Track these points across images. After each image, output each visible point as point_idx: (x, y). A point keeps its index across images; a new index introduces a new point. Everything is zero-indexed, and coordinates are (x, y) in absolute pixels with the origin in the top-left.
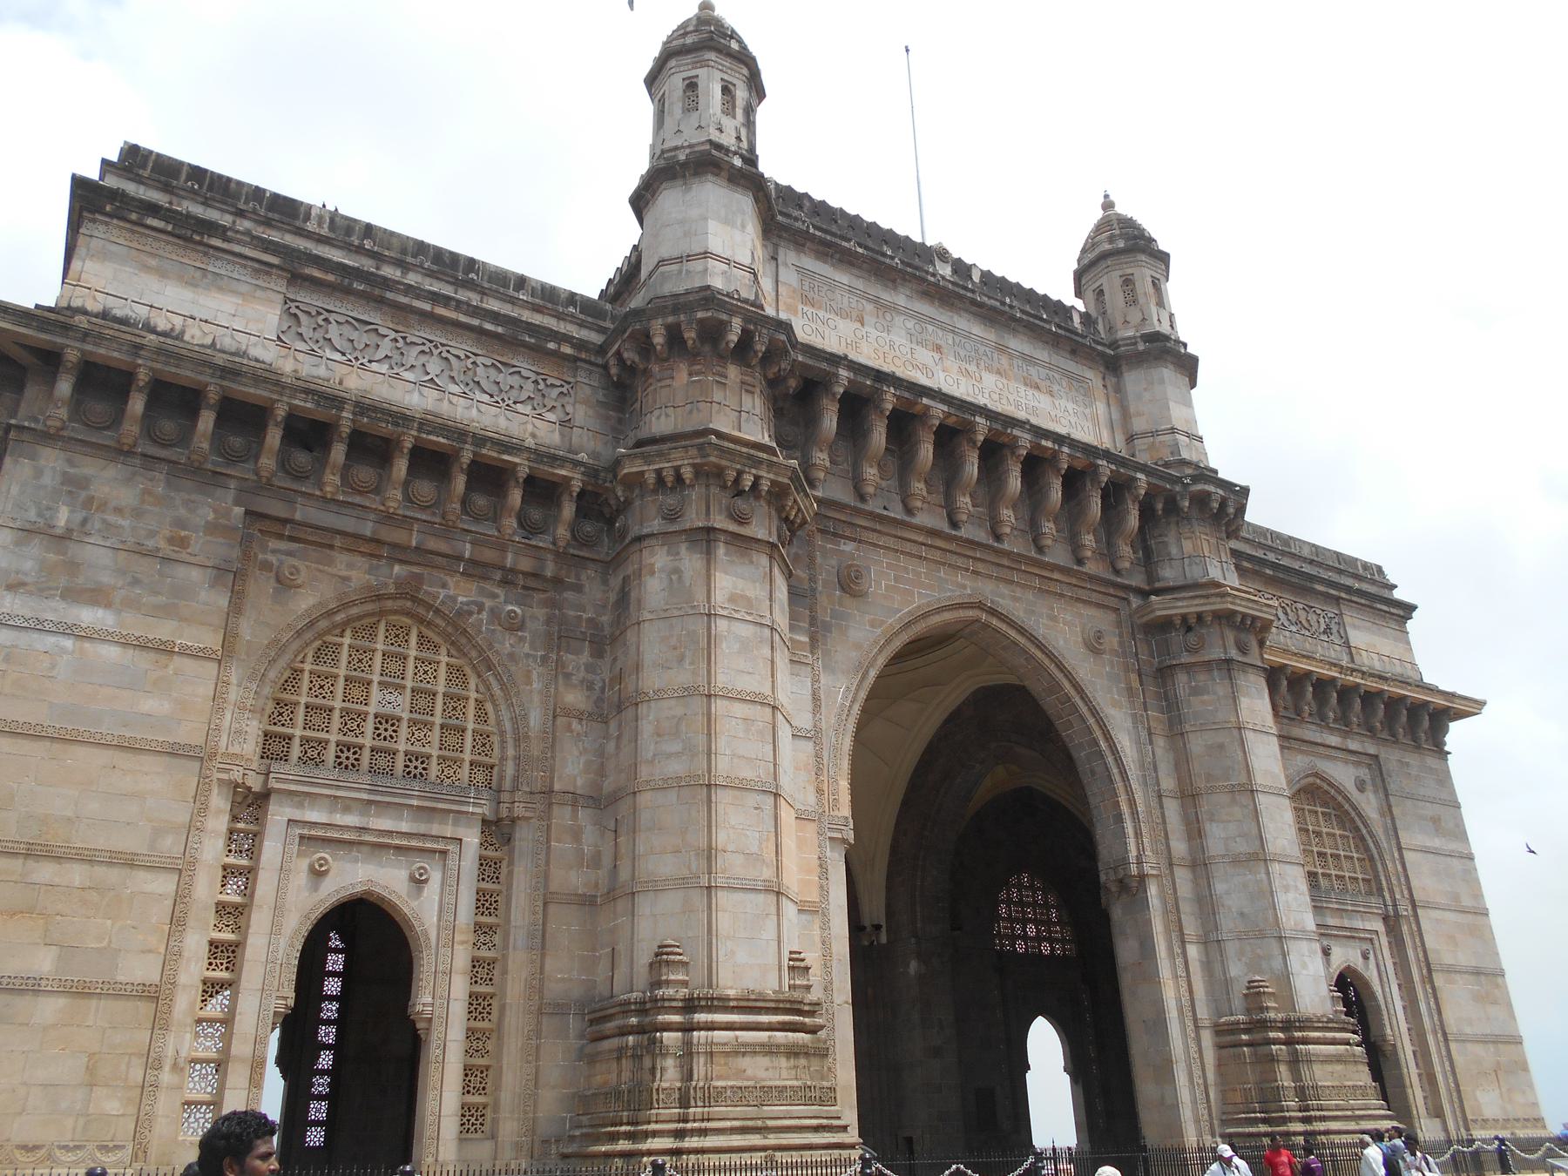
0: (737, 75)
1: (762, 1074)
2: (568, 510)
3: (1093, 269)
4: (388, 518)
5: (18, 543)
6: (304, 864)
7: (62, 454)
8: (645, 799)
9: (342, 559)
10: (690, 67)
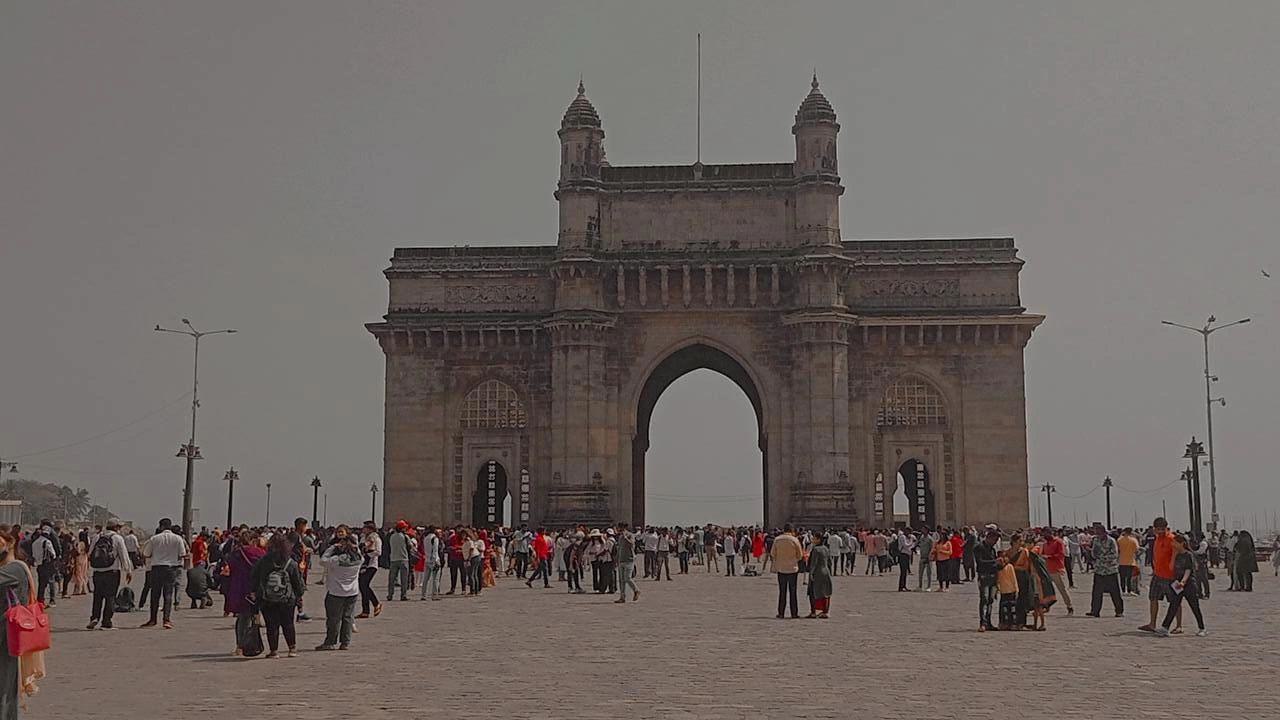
4: (483, 353)
6: (475, 454)
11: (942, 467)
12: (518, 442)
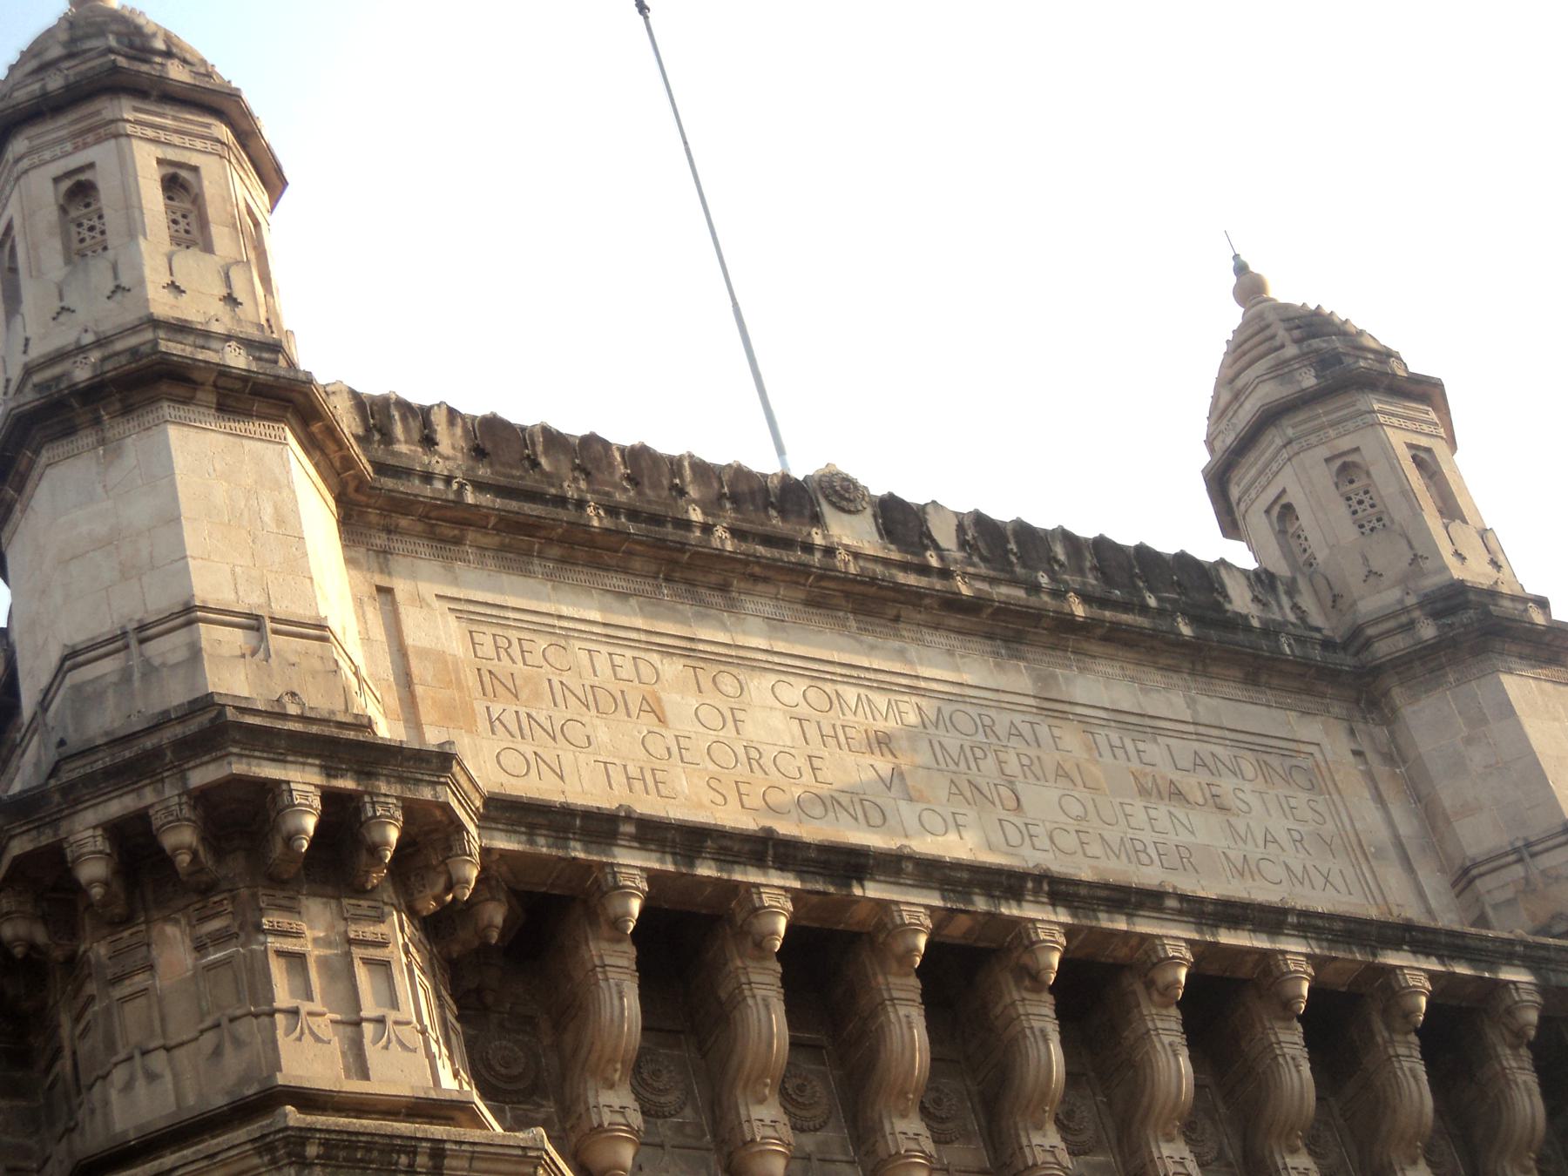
0: (199, 144)
3: (1252, 456)
10: (69, 147)
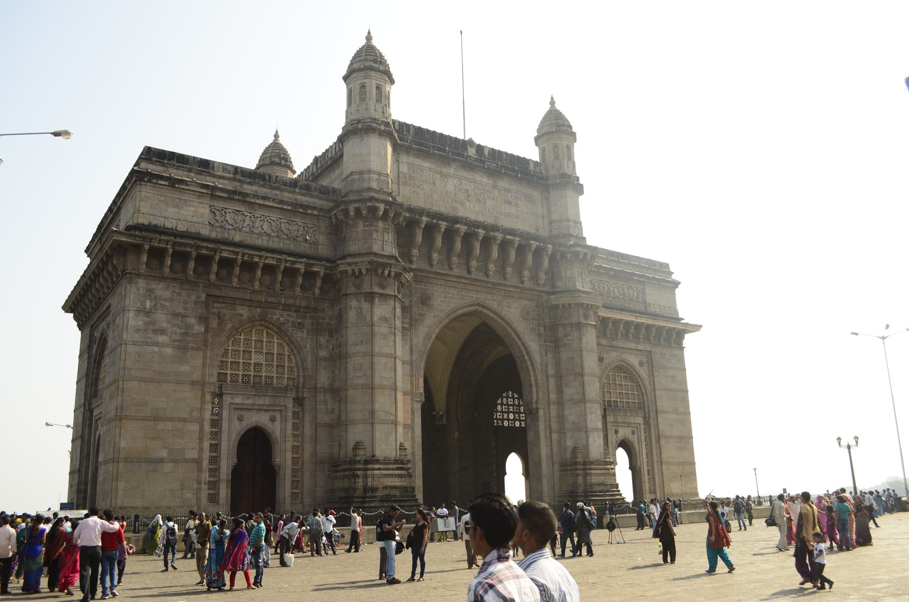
1: (390, 484)
2: (319, 283)
4: (254, 292)
5: (135, 316)
6: (236, 417)
7: (145, 281)
8: (350, 392)
9: (238, 307)
11: (644, 446)
12: (290, 405)
